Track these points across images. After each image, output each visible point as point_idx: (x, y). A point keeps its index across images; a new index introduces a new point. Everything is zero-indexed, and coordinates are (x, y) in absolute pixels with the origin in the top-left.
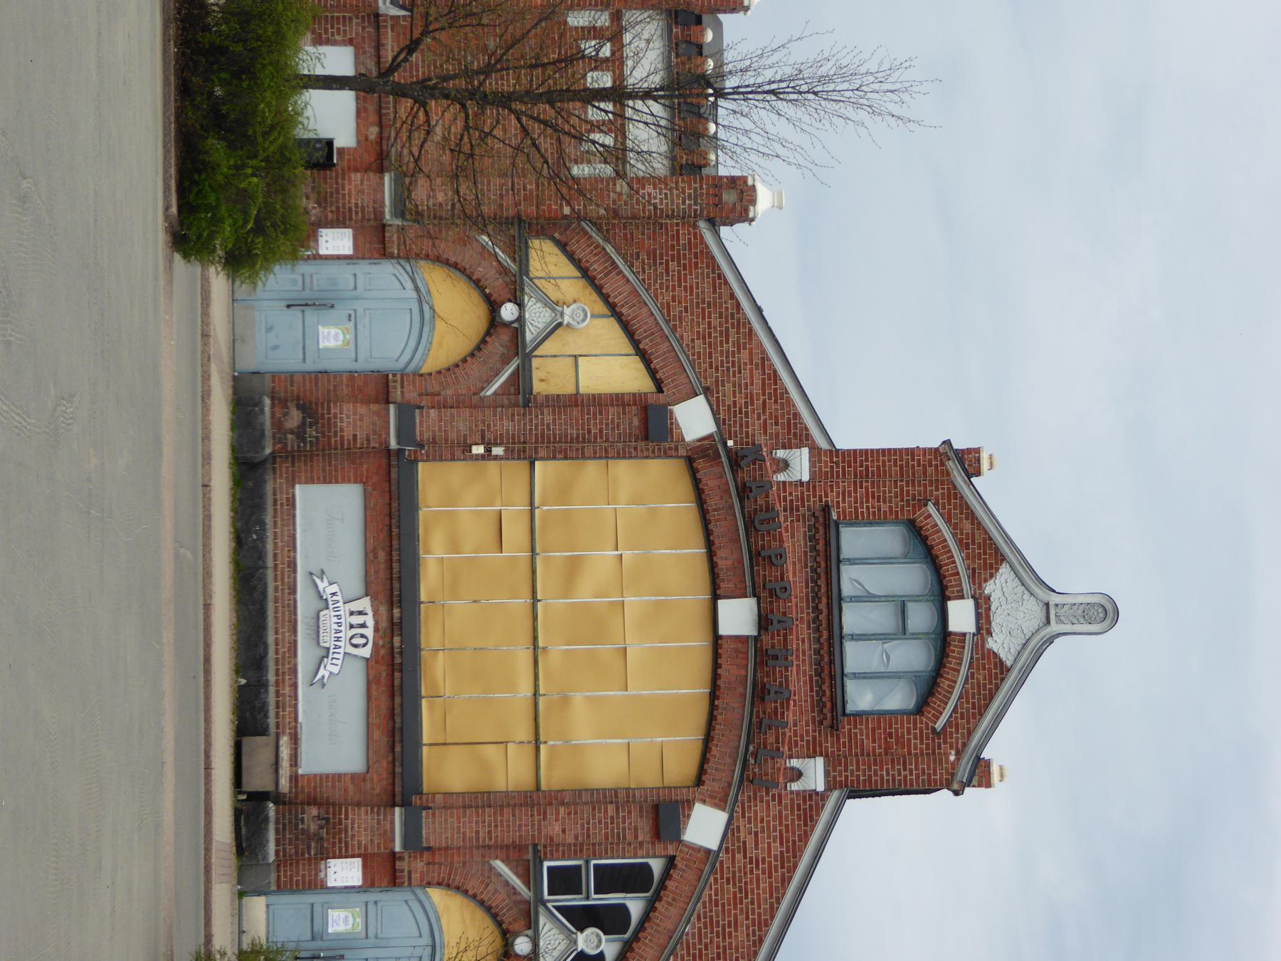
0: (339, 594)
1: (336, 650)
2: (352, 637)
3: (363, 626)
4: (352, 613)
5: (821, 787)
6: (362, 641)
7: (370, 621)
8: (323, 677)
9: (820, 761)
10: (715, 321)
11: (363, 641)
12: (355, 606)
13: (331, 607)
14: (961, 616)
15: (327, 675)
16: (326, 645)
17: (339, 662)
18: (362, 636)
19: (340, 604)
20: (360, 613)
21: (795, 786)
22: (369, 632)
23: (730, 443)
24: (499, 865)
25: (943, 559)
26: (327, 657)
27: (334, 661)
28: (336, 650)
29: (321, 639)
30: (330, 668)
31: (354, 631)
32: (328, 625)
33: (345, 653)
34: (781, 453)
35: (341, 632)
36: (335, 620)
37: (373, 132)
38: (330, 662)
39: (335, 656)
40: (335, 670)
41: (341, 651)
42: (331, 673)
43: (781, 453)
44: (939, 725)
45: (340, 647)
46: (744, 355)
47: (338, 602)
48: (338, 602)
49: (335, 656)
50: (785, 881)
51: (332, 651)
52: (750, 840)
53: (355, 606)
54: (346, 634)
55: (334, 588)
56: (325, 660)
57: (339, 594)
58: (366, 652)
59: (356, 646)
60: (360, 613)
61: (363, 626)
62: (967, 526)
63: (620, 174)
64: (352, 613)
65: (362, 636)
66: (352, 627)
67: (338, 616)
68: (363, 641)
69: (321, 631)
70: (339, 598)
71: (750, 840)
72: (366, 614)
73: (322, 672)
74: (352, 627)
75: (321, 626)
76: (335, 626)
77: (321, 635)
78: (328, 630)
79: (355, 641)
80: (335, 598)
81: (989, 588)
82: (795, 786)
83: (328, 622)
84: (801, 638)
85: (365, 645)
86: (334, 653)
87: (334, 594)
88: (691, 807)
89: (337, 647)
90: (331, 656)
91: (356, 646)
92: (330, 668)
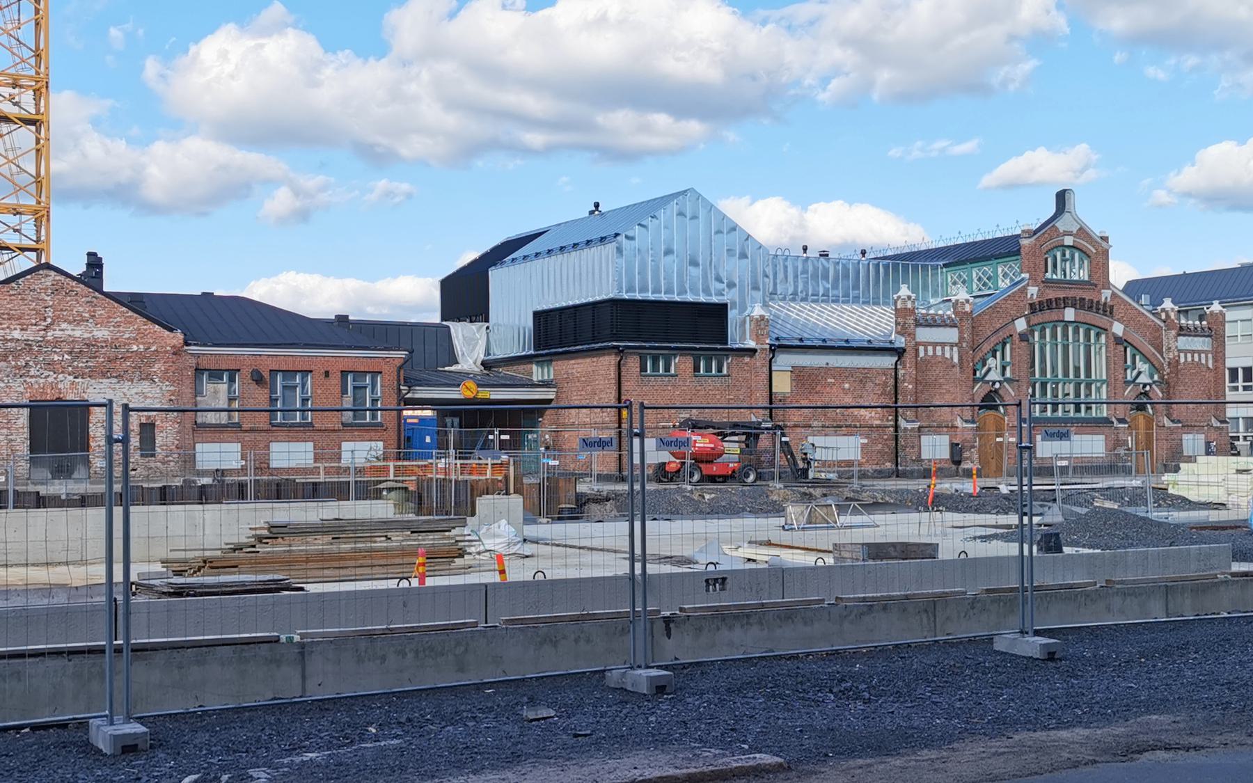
5: (1111, 292)
9: (1103, 291)
10: (994, 315)
14: (1069, 241)
21: (1109, 300)
23: (1026, 313)
24: (1126, 394)
25: (1054, 245)
34: (1029, 296)
37: (945, 429)
43: (1029, 296)
44: (1094, 251)
46: (1003, 306)
50: (1130, 305)
52: (1121, 315)
62: (1046, 235)
63: (956, 345)
71: (1121, 315)
81: (1061, 231)
82: (1109, 300)
84: (1078, 294)
88: (1113, 334)
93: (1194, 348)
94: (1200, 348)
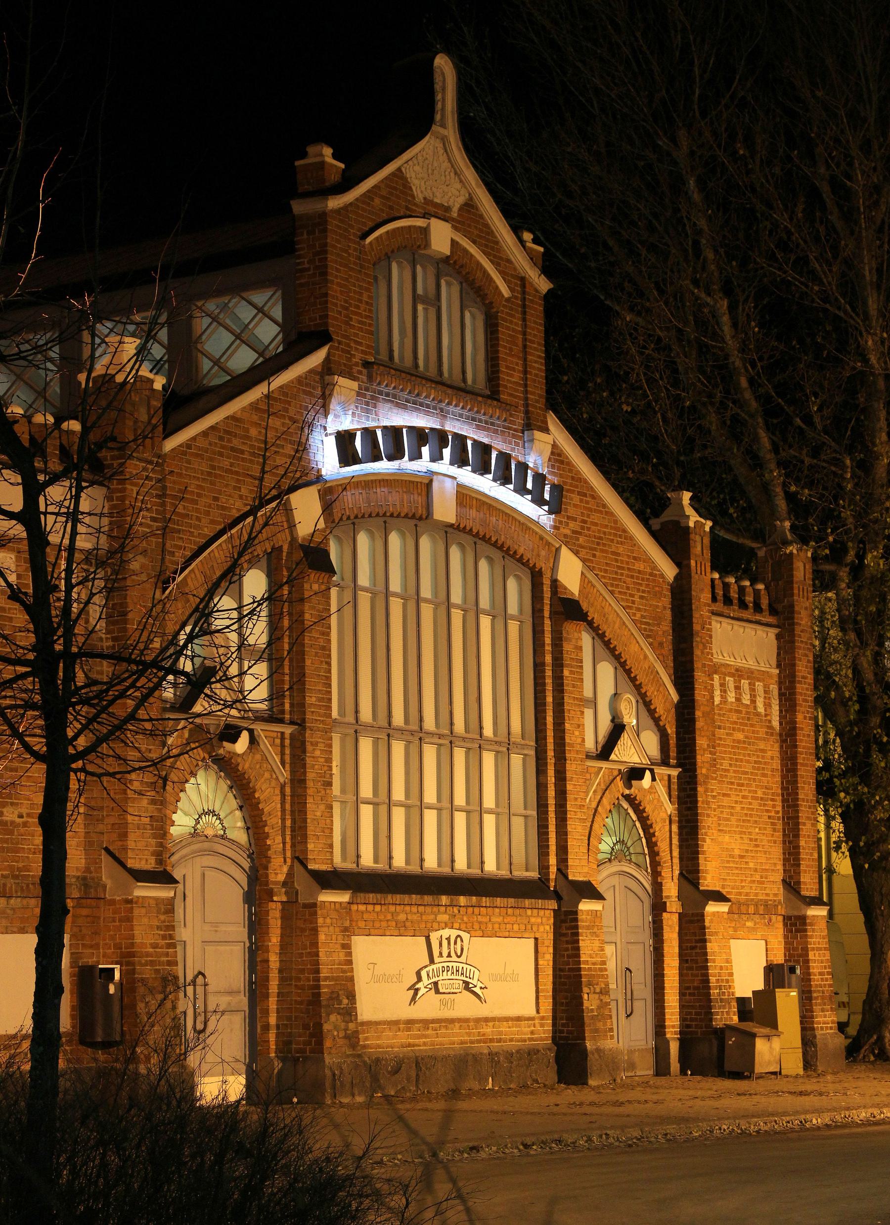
3: (448, 939)
4: (441, 955)
7: (446, 933)
15: (480, 985)
18: (455, 943)
22: (454, 933)
29: (455, 991)
31: (453, 954)
36: (445, 973)
51: (465, 979)
53: (436, 953)
56: (471, 986)
57: (427, 969)
58: (465, 936)
59: (462, 950)
61: (448, 939)
64: (441, 955)
65: (455, 943)
66: (449, 956)
68: (459, 939)
73: (477, 990)
74: (449, 956)
89: (462, 974)
90: (468, 980)
91: (462, 950)
93: (740, 663)
94: (751, 664)
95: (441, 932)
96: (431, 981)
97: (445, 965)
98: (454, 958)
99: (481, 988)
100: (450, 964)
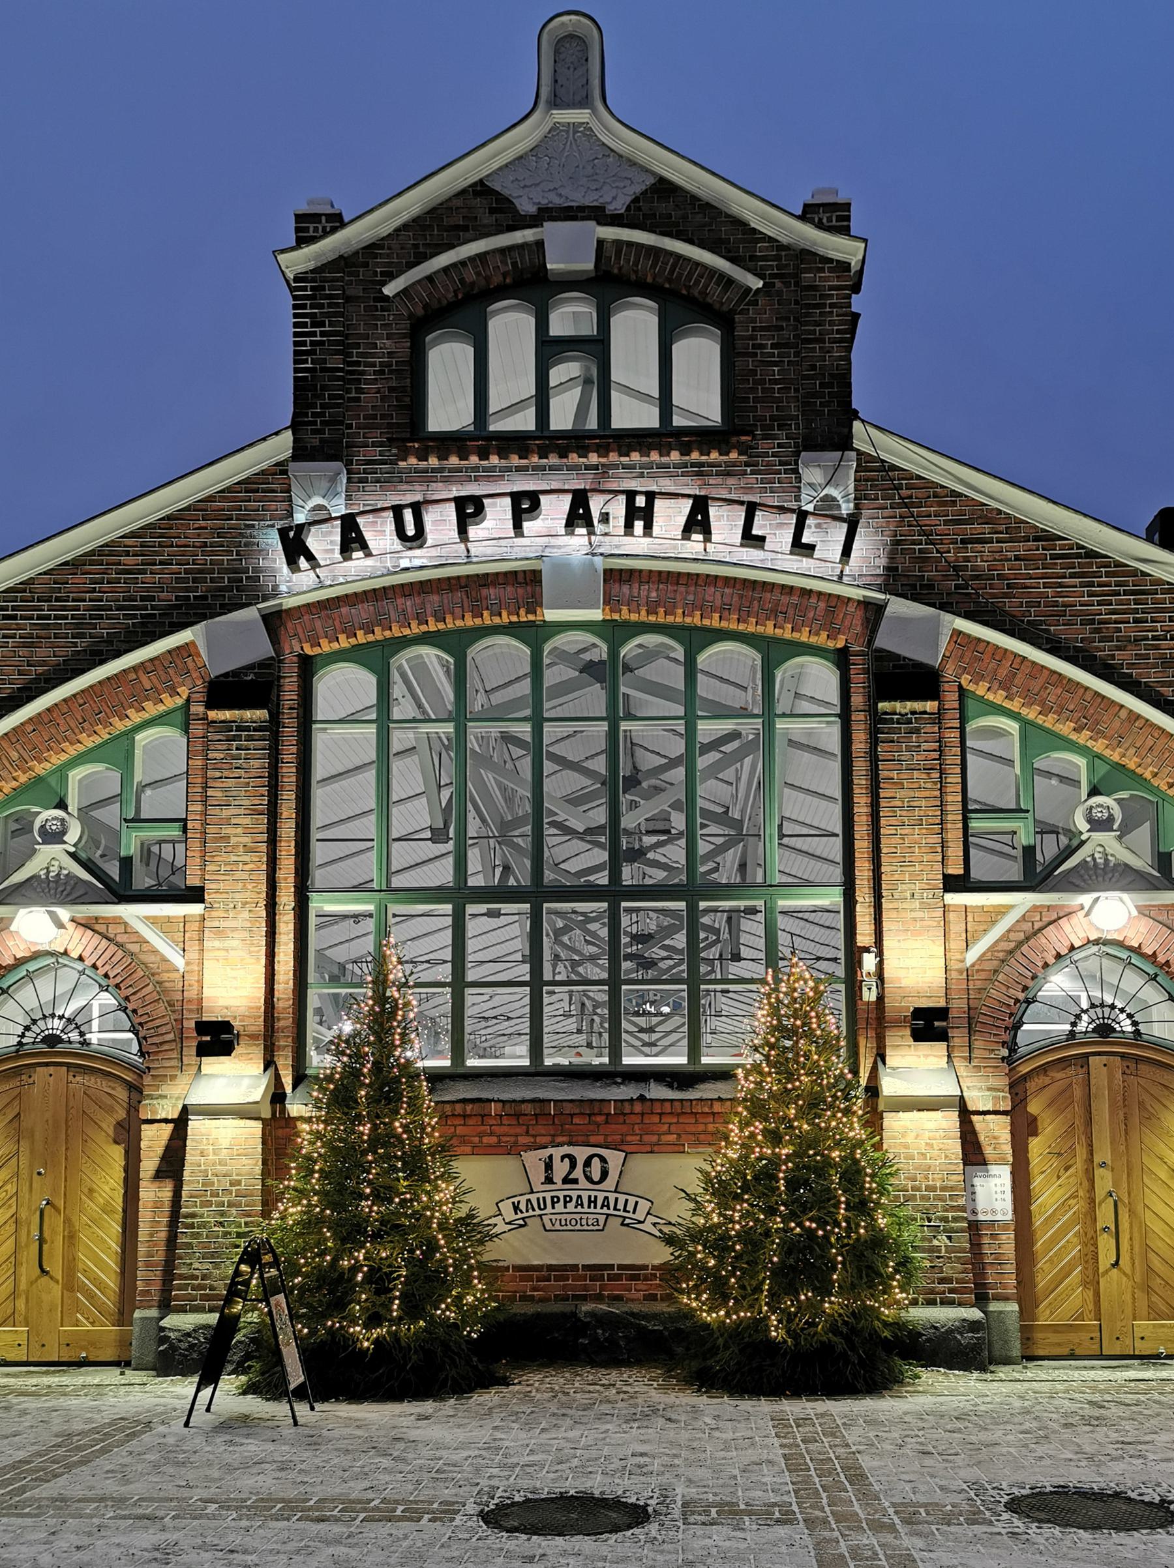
0: (515, 1200)
1: (612, 1206)
2: (589, 1179)
4: (549, 1180)
6: (596, 1163)
8: (654, 1224)
11: (596, 1161)
12: (538, 1176)
13: (538, 1212)
15: (651, 1219)
16: (602, 1219)
17: (632, 1200)
18: (588, 1163)
19: (533, 1197)
20: (549, 1166)
22: (581, 1153)
26: (625, 1218)
27: (630, 1207)
28: (612, 1206)
29: (591, 1228)
30: (640, 1215)
32: (569, 1217)
33: (616, 1191)
35: (579, 1197)
36: (559, 1207)
38: (630, 1215)
39: (620, 1206)
40: (644, 1206)
41: (612, 1197)
42: (648, 1213)
45: (606, 1198)
47: (529, 1201)
48: (529, 1201)
49: (620, 1206)
51: (612, 1212)
54: (584, 1189)
55: (507, 1208)
57: (515, 1200)
58: (615, 1158)
59: (605, 1174)
60: (549, 1166)
64: (549, 1180)
65: (588, 1163)
67: (553, 1203)
68: (596, 1161)
69: (578, 1227)
70: (523, 1199)
72: (551, 1157)
75: (569, 1227)
76: (571, 1207)
77: (586, 1227)
78: (577, 1217)
79: (596, 1177)
80: (523, 1207)
83: (563, 1217)
85: (603, 1160)
86: (615, 1209)
87: (516, 1208)
90: (621, 1213)
91: (605, 1174)
92: (640, 1215)
95: (550, 1151)
96: (520, 1215)
97: (561, 1194)
98: (583, 1183)
99: (654, 1224)
100: (574, 1194)
